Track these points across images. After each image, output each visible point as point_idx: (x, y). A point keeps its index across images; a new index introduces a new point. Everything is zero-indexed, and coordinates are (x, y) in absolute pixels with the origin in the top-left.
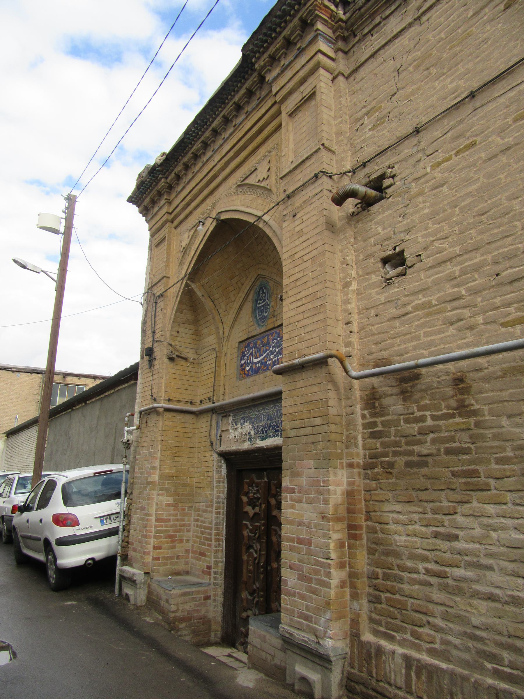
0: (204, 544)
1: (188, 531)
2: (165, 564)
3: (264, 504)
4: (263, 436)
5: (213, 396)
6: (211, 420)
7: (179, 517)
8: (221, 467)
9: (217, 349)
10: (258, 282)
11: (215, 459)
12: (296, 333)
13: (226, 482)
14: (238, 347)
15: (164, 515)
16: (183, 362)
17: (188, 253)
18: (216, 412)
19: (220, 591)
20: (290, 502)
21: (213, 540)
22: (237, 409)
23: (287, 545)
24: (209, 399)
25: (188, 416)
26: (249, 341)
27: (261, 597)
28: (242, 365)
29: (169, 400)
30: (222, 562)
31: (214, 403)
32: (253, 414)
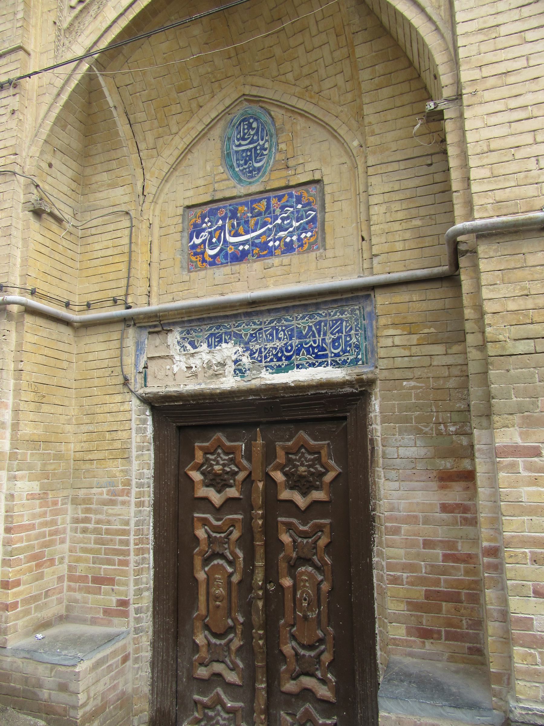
0: (109, 562)
1: (62, 541)
2: (27, 612)
3: (260, 481)
4: (280, 366)
5: (127, 295)
6: (122, 339)
7: (48, 519)
8: (144, 422)
9: (132, 213)
10: (238, 108)
11: (134, 408)
12: (513, 167)
13: (152, 448)
14: (183, 215)
15: (26, 518)
16: (54, 226)
17: (92, 13)
18: (135, 324)
19: (146, 640)
20: (524, 474)
21: (132, 553)
22: (199, 320)
23: (524, 553)
24: (115, 301)
25: (63, 328)
26: (214, 206)
27: (260, 639)
28: (194, 246)
29: (33, 293)
30: (148, 589)
31: (129, 307)
32: (246, 328)
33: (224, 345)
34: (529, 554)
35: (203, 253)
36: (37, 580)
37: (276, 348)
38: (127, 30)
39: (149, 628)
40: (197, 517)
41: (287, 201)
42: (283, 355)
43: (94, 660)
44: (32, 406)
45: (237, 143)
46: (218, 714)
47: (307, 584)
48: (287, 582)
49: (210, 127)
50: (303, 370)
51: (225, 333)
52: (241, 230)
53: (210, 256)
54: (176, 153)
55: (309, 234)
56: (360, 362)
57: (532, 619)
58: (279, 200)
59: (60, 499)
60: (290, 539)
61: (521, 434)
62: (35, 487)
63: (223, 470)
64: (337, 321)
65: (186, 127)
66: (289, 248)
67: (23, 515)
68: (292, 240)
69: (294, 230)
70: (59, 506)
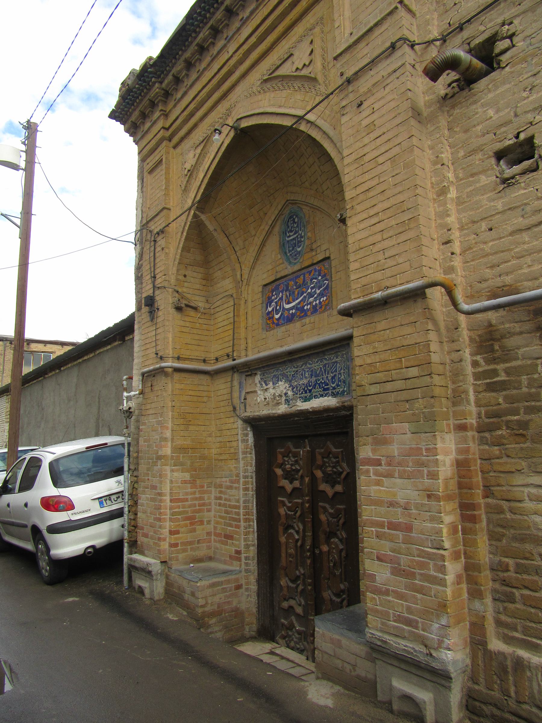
0: (231, 525)
1: (209, 510)
2: (185, 550)
3: (307, 477)
4: (306, 397)
5: (233, 351)
6: (232, 381)
7: (197, 495)
8: (247, 435)
9: (234, 295)
10: (286, 210)
11: (240, 426)
12: (370, 260)
13: (254, 452)
14: (262, 292)
15: (181, 494)
16: (192, 313)
17: (194, 177)
18: (238, 371)
19: (253, 578)
20: (373, 477)
21: (242, 521)
22: (267, 366)
23: (372, 531)
24: (228, 356)
25: (202, 377)
26: (277, 283)
27: (309, 585)
28: (269, 313)
29: (178, 358)
30: (253, 545)
31: (234, 360)
32: (290, 370)
33: (280, 383)
34: (374, 532)
35: (273, 317)
36: (191, 532)
37: (304, 384)
38: (209, 184)
39: (254, 570)
40: (280, 500)
41: (314, 275)
42: (308, 389)
43: (210, 582)
44: (182, 427)
45: (288, 235)
46: (293, 634)
47: (334, 551)
48: (325, 548)
49: (272, 226)
50: (317, 399)
51: (280, 374)
52: (291, 300)
53: (276, 319)
54: (257, 248)
55: (325, 298)
56: (346, 393)
57: (375, 575)
58: (310, 274)
59: (205, 484)
60: (326, 518)
61: (372, 450)
62: (187, 476)
63: (291, 468)
64: (334, 363)
65: (260, 230)
66: (315, 310)
67: (179, 493)
68: (316, 304)
69: (317, 297)
70: (205, 488)
